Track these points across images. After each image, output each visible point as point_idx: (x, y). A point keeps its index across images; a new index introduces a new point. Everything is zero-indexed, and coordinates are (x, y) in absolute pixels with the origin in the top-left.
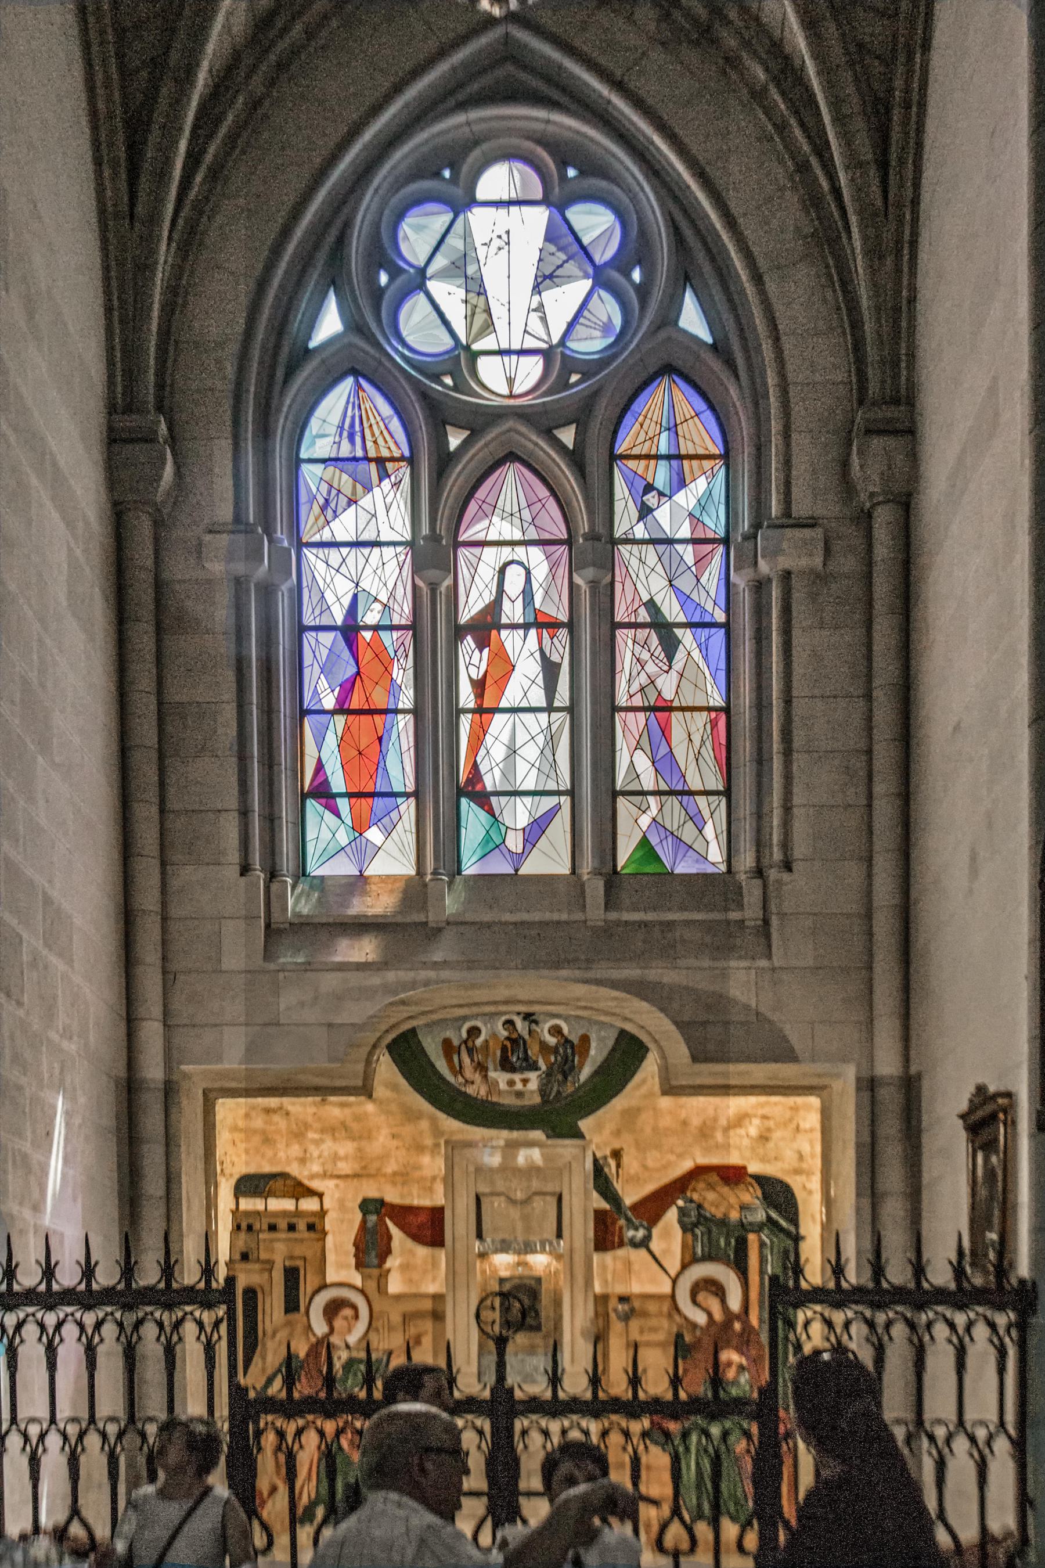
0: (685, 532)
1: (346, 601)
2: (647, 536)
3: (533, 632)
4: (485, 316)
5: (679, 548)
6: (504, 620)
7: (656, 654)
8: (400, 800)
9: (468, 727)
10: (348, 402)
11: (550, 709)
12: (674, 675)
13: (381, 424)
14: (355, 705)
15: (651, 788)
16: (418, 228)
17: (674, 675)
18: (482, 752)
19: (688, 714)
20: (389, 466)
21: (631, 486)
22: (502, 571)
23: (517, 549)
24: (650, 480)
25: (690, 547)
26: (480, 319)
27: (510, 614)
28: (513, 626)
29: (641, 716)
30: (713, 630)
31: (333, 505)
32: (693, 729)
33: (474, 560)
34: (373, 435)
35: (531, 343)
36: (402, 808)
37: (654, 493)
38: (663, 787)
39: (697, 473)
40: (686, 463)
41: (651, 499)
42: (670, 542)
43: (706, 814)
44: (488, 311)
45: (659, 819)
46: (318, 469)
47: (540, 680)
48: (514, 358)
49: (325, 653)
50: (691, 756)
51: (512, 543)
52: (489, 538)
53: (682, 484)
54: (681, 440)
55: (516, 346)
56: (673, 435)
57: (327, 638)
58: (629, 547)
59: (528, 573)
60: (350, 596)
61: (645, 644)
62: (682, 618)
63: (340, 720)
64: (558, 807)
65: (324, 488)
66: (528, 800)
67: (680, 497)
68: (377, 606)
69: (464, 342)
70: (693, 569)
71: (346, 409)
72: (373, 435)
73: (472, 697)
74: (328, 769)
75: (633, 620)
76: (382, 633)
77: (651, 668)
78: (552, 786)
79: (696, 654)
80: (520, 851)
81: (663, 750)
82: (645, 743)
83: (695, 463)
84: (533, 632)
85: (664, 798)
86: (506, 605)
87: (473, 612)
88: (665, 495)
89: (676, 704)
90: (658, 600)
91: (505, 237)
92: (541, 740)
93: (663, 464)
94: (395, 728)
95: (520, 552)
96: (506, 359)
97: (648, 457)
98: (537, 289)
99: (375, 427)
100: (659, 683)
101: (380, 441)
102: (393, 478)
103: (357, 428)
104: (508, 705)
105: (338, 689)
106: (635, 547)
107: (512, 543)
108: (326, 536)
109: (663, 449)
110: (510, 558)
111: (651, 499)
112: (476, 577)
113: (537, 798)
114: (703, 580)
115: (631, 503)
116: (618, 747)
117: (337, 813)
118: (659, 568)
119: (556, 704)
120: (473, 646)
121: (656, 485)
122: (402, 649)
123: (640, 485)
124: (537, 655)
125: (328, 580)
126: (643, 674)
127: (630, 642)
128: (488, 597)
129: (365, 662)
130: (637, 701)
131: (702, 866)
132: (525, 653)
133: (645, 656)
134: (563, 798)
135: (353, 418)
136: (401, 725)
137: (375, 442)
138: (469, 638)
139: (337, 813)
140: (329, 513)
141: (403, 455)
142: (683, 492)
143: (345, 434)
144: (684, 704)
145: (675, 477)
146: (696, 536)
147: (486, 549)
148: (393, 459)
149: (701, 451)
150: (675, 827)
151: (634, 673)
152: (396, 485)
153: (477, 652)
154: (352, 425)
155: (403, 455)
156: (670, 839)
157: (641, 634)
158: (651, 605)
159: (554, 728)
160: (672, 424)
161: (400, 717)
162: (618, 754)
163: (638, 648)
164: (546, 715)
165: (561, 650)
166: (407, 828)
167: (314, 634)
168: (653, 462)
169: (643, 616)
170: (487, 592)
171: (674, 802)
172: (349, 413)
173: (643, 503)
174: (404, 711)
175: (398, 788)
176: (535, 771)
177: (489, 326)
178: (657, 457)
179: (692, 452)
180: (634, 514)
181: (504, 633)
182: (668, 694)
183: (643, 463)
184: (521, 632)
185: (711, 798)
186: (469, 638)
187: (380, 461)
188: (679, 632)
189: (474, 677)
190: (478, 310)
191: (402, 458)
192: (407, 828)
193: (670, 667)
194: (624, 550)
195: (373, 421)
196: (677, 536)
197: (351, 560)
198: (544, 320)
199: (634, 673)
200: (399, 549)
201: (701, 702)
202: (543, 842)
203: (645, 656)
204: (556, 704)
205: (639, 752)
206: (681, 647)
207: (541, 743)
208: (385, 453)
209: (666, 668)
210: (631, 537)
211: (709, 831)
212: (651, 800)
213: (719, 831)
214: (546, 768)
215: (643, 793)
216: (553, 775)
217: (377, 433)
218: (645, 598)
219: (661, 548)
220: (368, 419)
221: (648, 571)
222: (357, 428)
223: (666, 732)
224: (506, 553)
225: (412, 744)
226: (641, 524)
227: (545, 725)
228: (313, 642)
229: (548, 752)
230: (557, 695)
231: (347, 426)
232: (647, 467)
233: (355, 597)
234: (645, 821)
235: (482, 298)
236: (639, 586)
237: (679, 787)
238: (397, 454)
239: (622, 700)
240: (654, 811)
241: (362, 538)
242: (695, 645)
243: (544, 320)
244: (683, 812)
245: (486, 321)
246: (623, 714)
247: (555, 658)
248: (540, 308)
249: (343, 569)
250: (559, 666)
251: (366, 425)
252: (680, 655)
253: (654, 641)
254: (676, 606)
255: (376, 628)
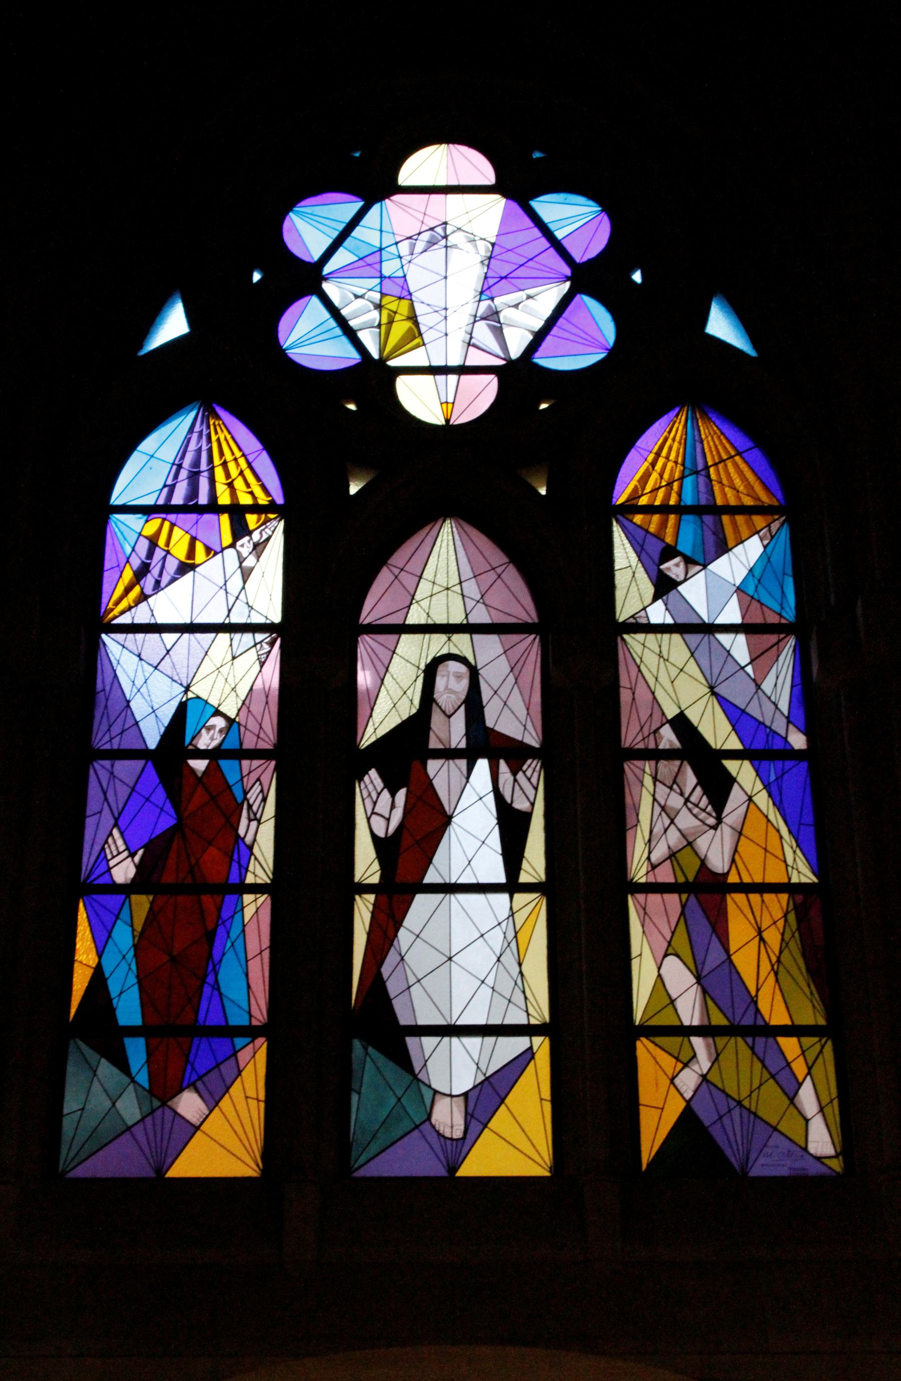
0: (732, 614)
1: (167, 714)
2: (669, 620)
3: (482, 766)
4: (408, 324)
5: (725, 639)
6: (434, 744)
7: (694, 799)
8: (239, 1042)
9: (367, 917)
10: (191, 430)
11: (512, 886)
12: (726, 833)
13: (242, 461)
14: (169, 878)
15: (696, 1022)
16: (313, 219)
17: (726, 833)
18: (391, 959)
19: (755, 898)
20: (251, 519)
21: (640, 550)
22: (431, 671)
23: (456, 637)
24: (669, 539)
25: (741, 638)
26: (400, 328)
27: (442, 736)
28: (449, 754)
29: (673, 900)
30: (788, 764)
31: (155, 571)
32: (766, 922)
33: (385, 657)
34: (228, 475)
35: (476, 359)
36: (243, 1056)
37: (677, 559)
38: (718, 1019)
39: (744, 531)
40: (725, 519)
41: (674, 568)
42: (710, 629)
43: (799, 1068)
44: (413, 318)
45: (714, 1077)
46: (134, 521)
47: (495, 840)
48: (453, 378)
49: (124, 792)
50: (766, 967)
51: (448, 629)
52: (410, 621)
53: (723, 548)
54: (716, 488)
55: (455, 361)
56: (702, 479)
57: (127, 769)
58: (640, 637)
59: (474, 673)
60: (174, 705)
61: (674, 783)
62: (734, 743)
63: (141, 903)
64: (529, 1055)
65: (143, 547)
66: (473, 1043)
67: (720, 566)
68: (219, 722)
69: (376, 356)
70: (749, 669)
71: (187, 441)
72: (228, 475)
73: (376, 866)
74: (114, 988)
75: (652, 746)
76: (224, 764)
77: (686, 821)
78: (517, 1018)
79: (763, 800)
80: (458, 1133)
81: (715, 956)
82: (682, 942)
83: (740, 519)
84: (482, 766)
85: (721, 1041)
86: (437, 719)
87: (381, 732)
88: (696, 563)
89: (733, 879)
90: (693, 716)
91: (439, 230)
92: (496, 939)
93: (689, 520)
94: (238, 916)
95: (461, 644)
96: (441, 378)
97: (664, 509)
98: (486, 291)
99: (232, 466)
100: (702, 844)
101: (239, 484)
102: (256, 536)
103: (204, 466)
104: (438, 880)
105: (141, 852)
106: (651, 637)
107: (448, 629)
108: (141, 615)
109: (688, 499)
110: (444, 651)
111: (674, 568)
112: (388, 679)
113: (490, 1040)
114: (767, 686)
115: (641, 574)
116: (635, 951)
117: (122, 1063)
118: (692, 667)
119: (524, 878)
120: (379, 783)
121: (680, 548)
122: (257, 787)
123: (655, 548)
124: (490, 799)
125: (139, 682)
126: (672, 830)
127: (648, 781)
128: (408, 708)
129: (186, 814)
130: (665, 875)
131: (799, 1164)
132: (469, 797)
133: (676, 801)
134: (537, 1041)
135: (199, 451)
136: (249, 912)
137: (231, 485)
138: (373, 773)
139: (122, 1063)
140: (149, 582)
141: (272, 502)
142: (725, 558)
143: (184, 474)
144: (747, 879)
145: (710, 539)
146: (748, 620)
147: (405, 637)
148: (255, 508)
149: (748, 501)
150: (744, 1093)
151: (658, 829)
152: (258, 548)
153: (386, 794)
154: (196, 463)
155: (272, 502)
156: (736, 1112)
157: (667, 768)
158: (681, 724)
159: (520, 918)
160: (700, 466)
161: (248, 898)
162: (635, 964)
163: (662, 790)
164: (505, 897)
165: (531, 792)
166: (252, 1093)
167: (107, 763)
168: (672, 518)
169: (668, 738)
170: (405, 701)
171: (738, 1047)
172: (193, 446)
173: (661, 573)
174: (256, 889)
175: (237, 1019)
176: (486, 991)
177: (415, 335)
178: (680, 510)
179: (733, 502)
180: (649, 590)
181: (433, 766)
182: (718, 862)
183: (656, 518)
184: (463, 763)
185: (807, 1041)
186: (373, 773)
187: (237, 512)
188: (731, 766)
189: (381, 834)
190: (397, 317)
191: (272, 507)
192: (252, 1093)
193: (719, 820)
194: (634, 641)
195: (228, 456)
196: (719, 621)
197: (180, 653)
198: (498, 332)
199: (658, 829)
200: (259, 637)
201: (775, 876)
202: (500, 1120)
203: (676, 801)
204: (524, 878)
205: (671, 960)
206: (736, 786)
207: (498, 946)
208: (245, 499)
209: (712, 821)
210: (644, 621)
211: (807, 1097)
212: (698, 1042)
213: (825, 1100)
214: (506, 987)
215: (688, 1031)
216: (518, 998)
217: (234, 472)
218: (671, 712)
219: (694, 639)
220: (222, 454)
221: (674, 672)
222: (204, 466)
223: (720, 929)
224: (437, 644)
225: (266, 943)
226: (660, 603)
227: (504, 913)
228: (104, 776)
229: (509, 960)
230: (525, 865)
231: (187, 463)
232: (663, 525)
233: (182, 708)
234: (688, 1081)
235: (405, 304)
236: (660, 695)
237: (748, 1021)
238: (263, 500)
239: (639, 872)
240: (704, 1062)
241: (199, 620)
242: (759, 785)
243: (498, 332)
244: (758, 1065)
245: (410, 329)
246: (641, 897)
247: (521, 804)
248: (493, 315)
249: (166, 665)
250: (526, 817)
251: (217, 461)
252: (736, 798)
253: (690, 779)
254: (724, 726)
255: (214, 755)
